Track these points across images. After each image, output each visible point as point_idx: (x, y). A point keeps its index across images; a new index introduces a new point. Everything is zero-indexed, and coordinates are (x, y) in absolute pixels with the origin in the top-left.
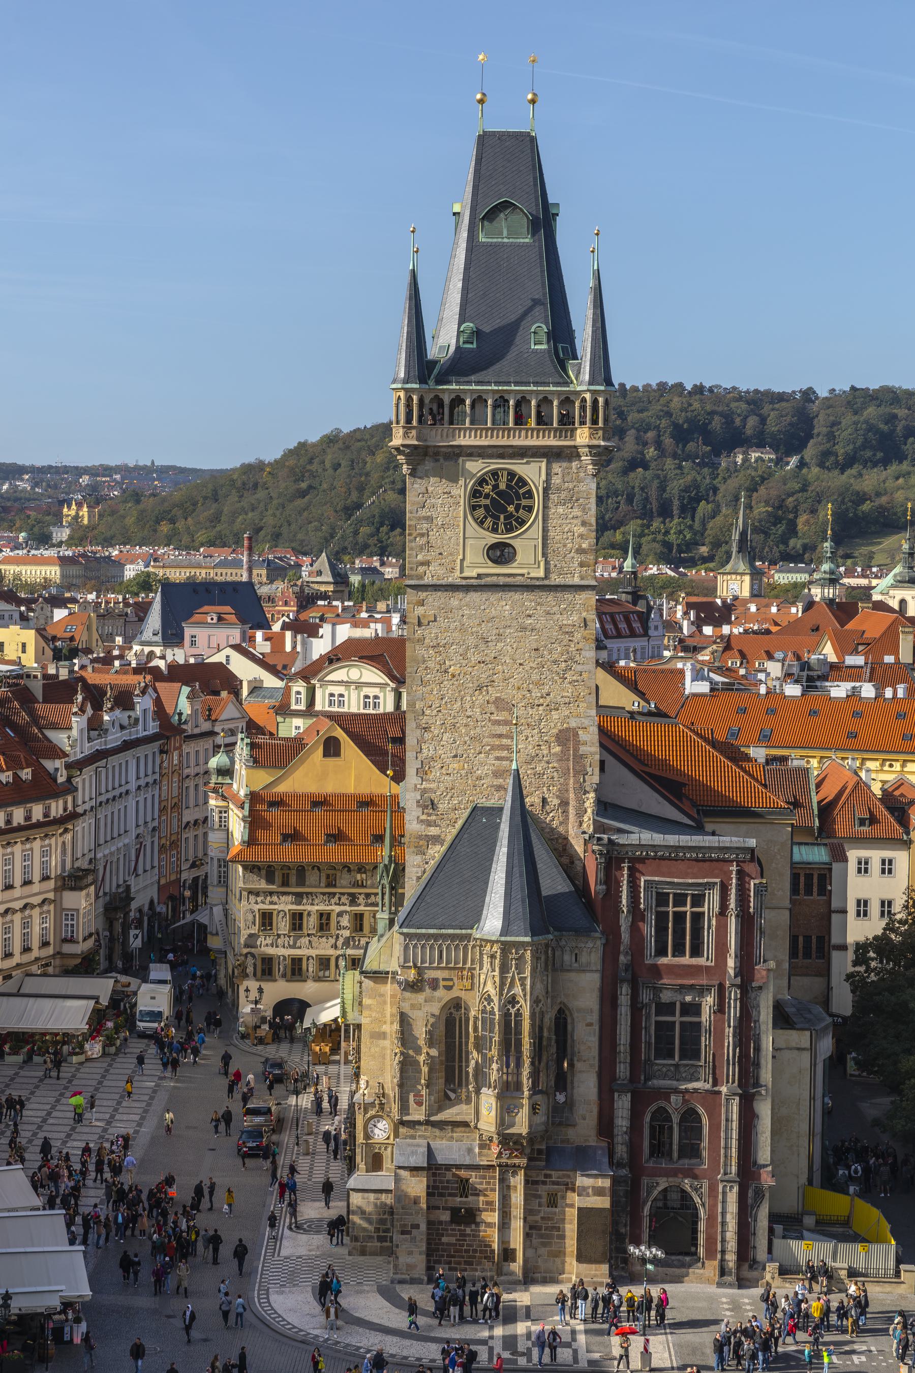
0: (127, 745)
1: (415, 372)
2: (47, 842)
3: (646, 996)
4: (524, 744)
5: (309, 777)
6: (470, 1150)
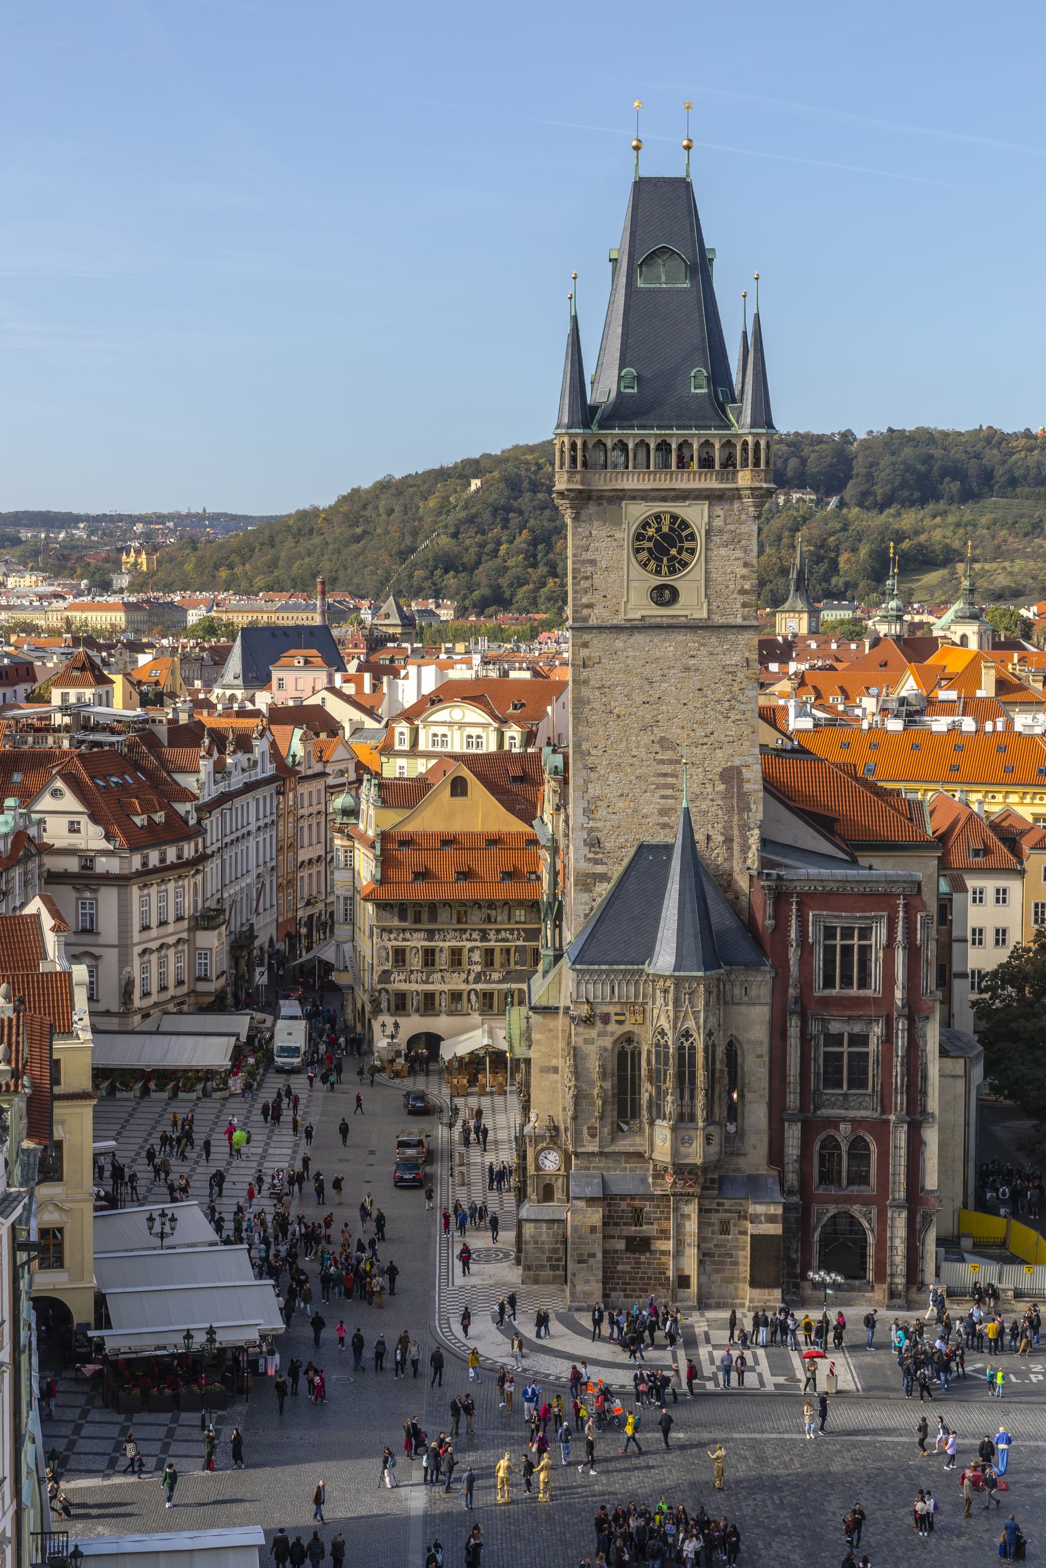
0: (249, 787)
1: (579, 417)
2: (180, 883)
3: (814, 1028)
4: (689, 783)
5: (436, 817)
6: (644, 1180)
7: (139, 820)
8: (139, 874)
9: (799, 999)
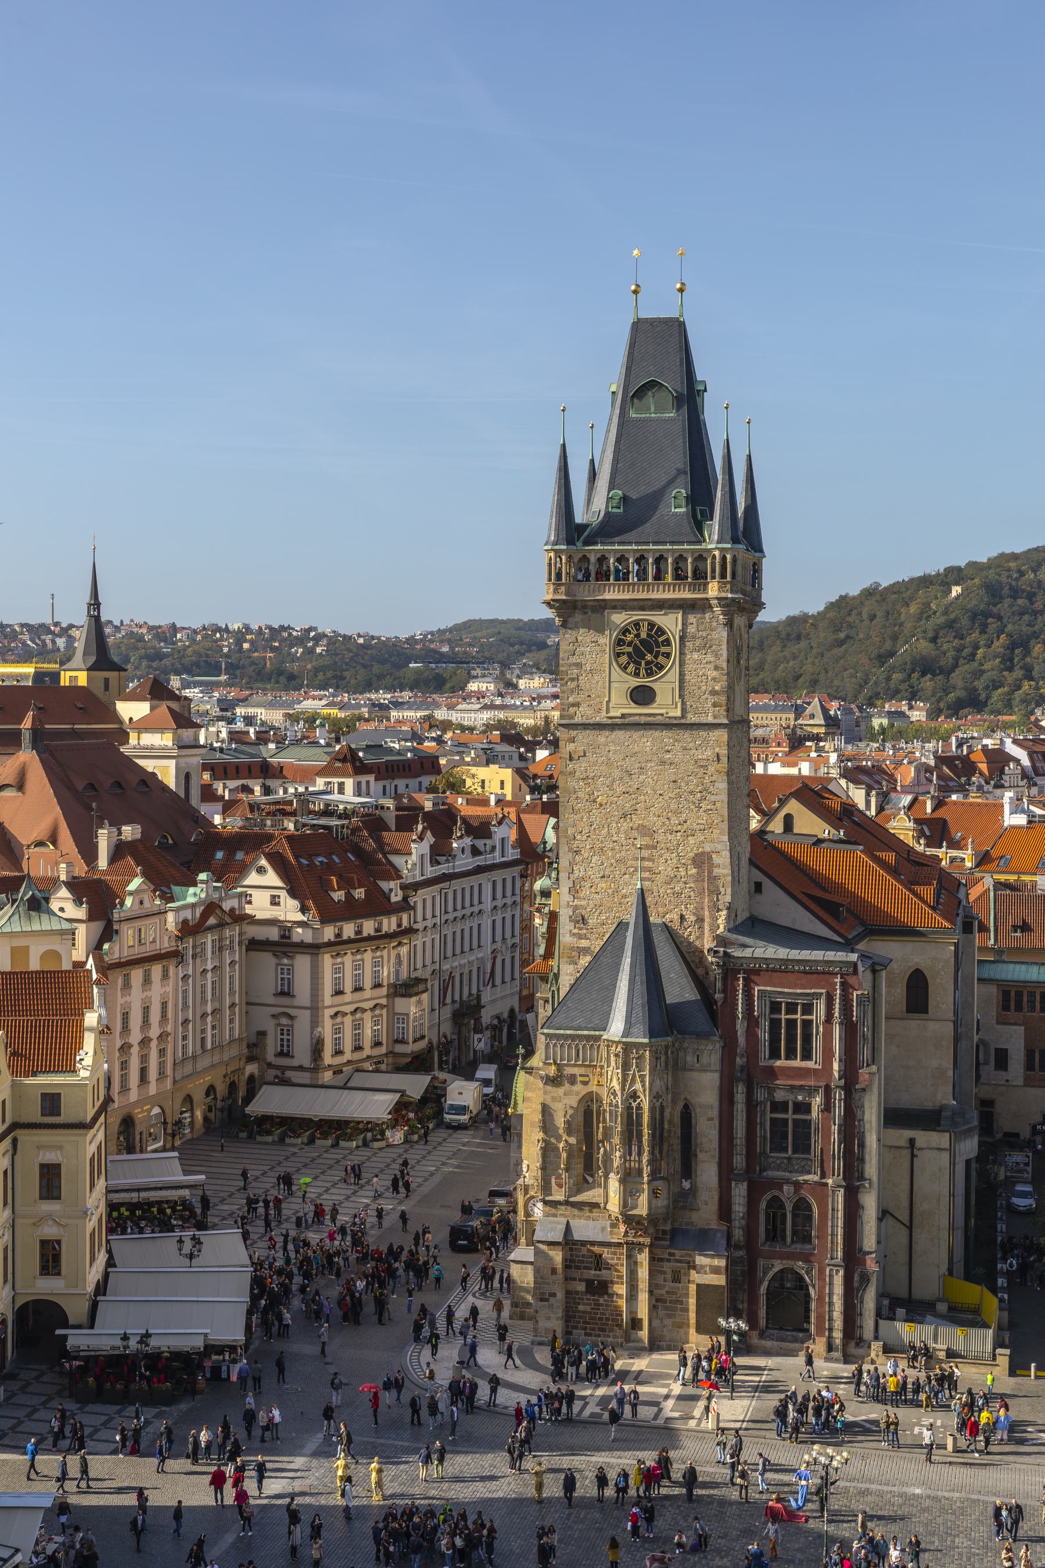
0: (479, 870)
2: (378, 954)
3: (760, 1095)
6: (603, 1229)
7: (338, 896)
8: (330, 944)
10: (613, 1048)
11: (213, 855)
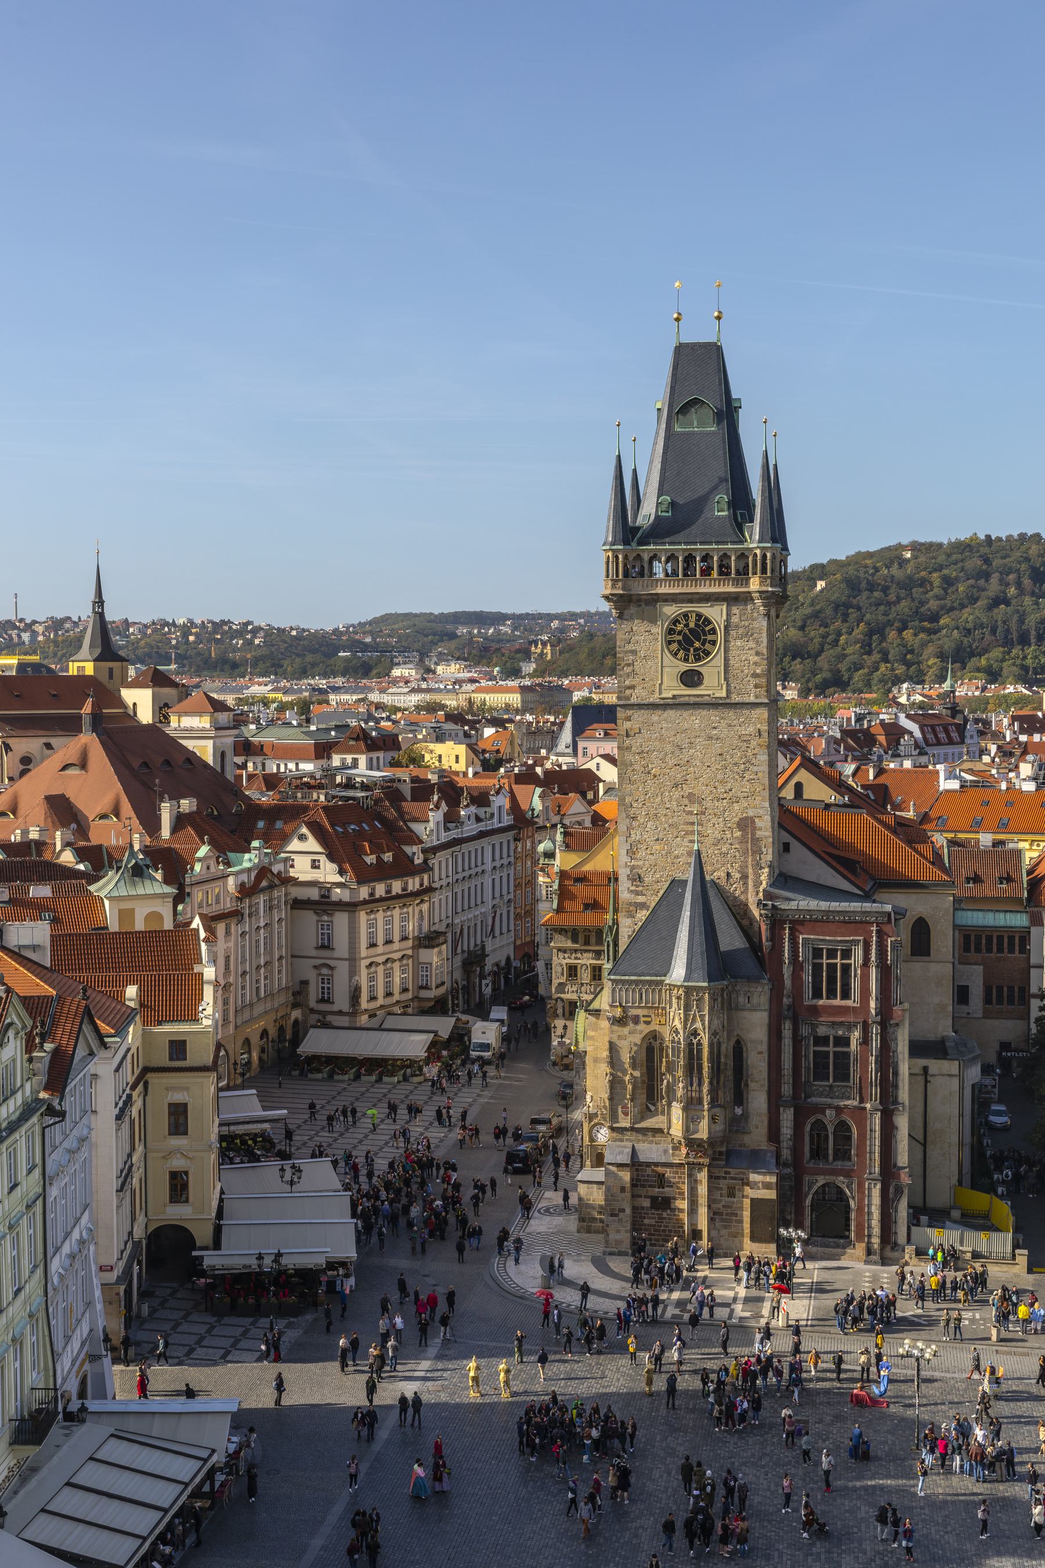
0: (482, 835)
1: (620, 536)
2: (405, 910)
3: (805, 1031)
6: (666, 1151)
7: (370, 859)
8: (365, 902)
9: (791, 1007)
10: (675, 991)
11: (255, 824)
